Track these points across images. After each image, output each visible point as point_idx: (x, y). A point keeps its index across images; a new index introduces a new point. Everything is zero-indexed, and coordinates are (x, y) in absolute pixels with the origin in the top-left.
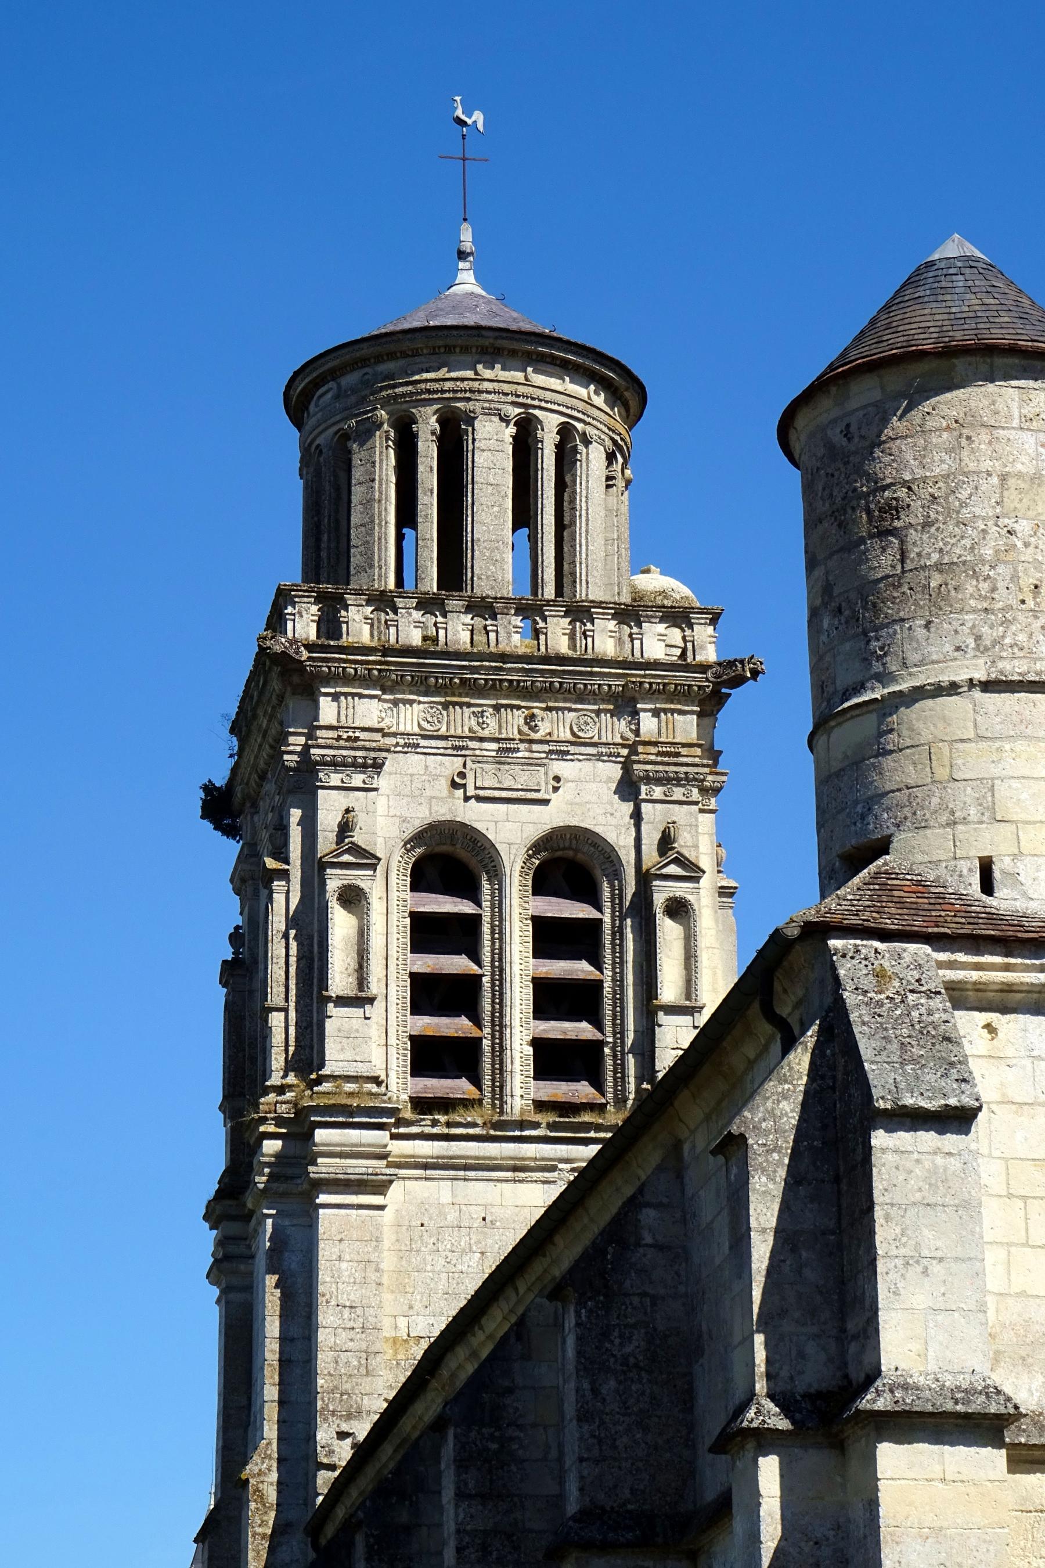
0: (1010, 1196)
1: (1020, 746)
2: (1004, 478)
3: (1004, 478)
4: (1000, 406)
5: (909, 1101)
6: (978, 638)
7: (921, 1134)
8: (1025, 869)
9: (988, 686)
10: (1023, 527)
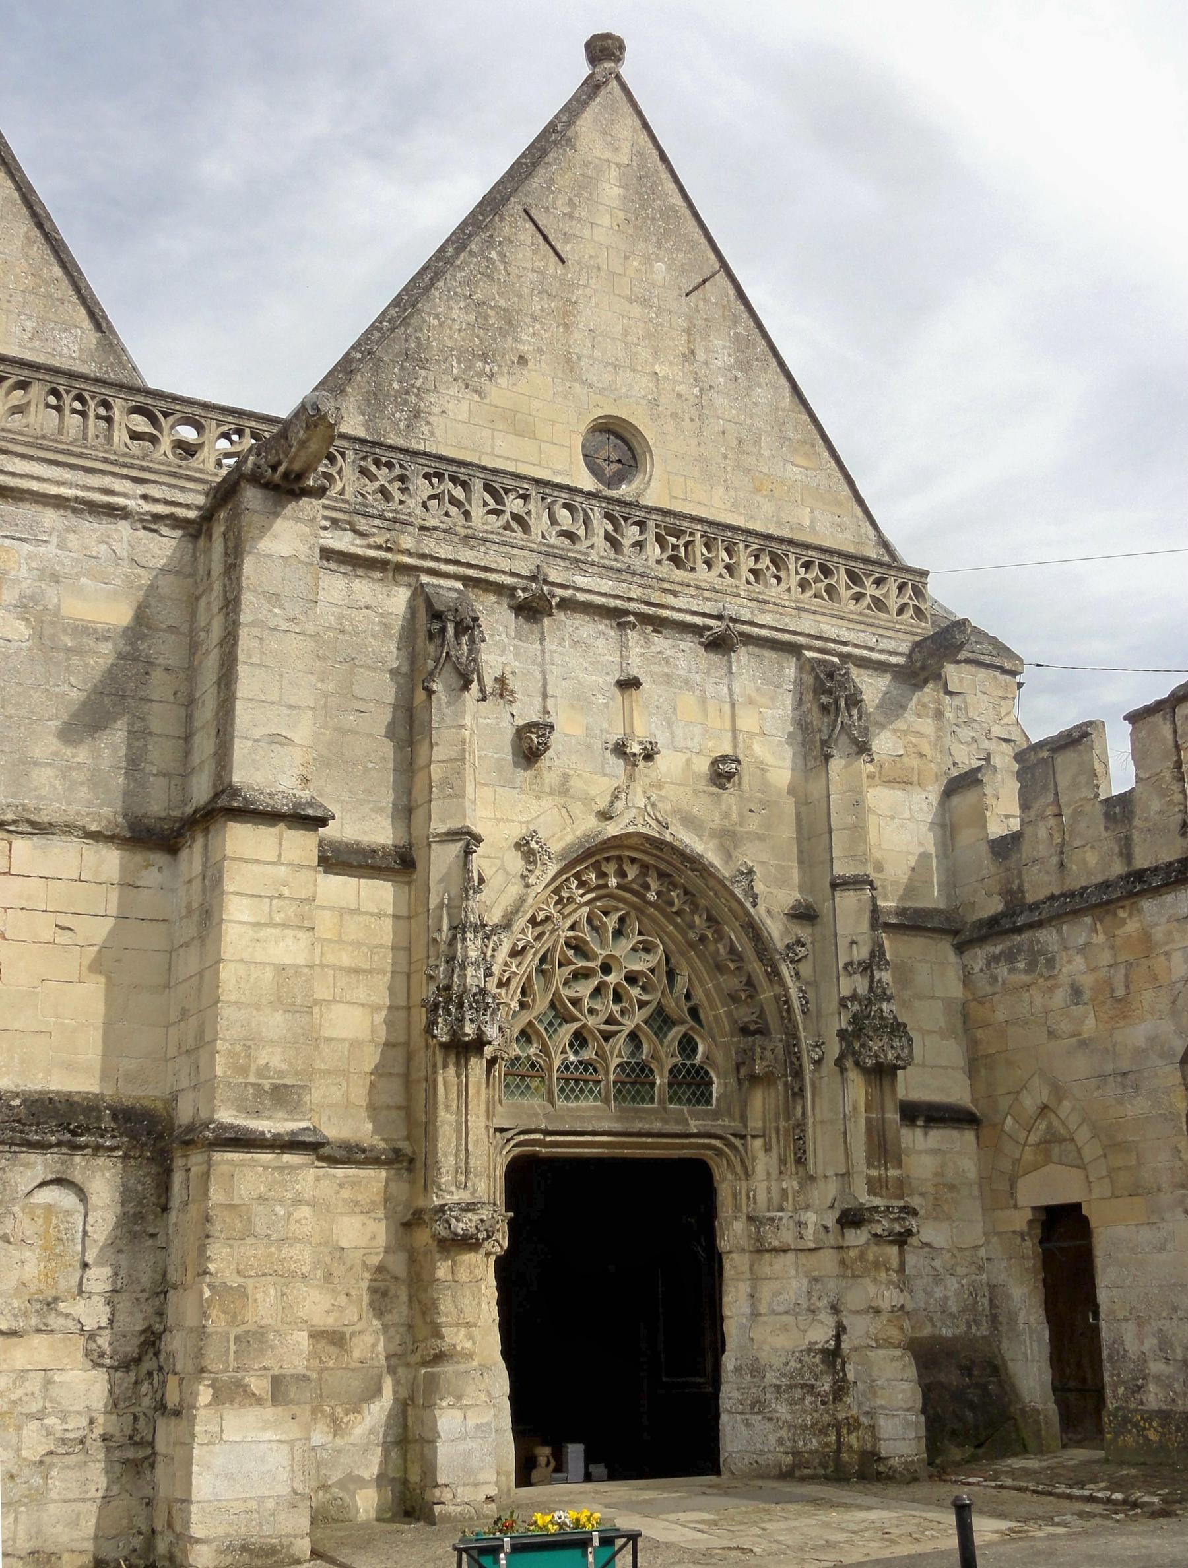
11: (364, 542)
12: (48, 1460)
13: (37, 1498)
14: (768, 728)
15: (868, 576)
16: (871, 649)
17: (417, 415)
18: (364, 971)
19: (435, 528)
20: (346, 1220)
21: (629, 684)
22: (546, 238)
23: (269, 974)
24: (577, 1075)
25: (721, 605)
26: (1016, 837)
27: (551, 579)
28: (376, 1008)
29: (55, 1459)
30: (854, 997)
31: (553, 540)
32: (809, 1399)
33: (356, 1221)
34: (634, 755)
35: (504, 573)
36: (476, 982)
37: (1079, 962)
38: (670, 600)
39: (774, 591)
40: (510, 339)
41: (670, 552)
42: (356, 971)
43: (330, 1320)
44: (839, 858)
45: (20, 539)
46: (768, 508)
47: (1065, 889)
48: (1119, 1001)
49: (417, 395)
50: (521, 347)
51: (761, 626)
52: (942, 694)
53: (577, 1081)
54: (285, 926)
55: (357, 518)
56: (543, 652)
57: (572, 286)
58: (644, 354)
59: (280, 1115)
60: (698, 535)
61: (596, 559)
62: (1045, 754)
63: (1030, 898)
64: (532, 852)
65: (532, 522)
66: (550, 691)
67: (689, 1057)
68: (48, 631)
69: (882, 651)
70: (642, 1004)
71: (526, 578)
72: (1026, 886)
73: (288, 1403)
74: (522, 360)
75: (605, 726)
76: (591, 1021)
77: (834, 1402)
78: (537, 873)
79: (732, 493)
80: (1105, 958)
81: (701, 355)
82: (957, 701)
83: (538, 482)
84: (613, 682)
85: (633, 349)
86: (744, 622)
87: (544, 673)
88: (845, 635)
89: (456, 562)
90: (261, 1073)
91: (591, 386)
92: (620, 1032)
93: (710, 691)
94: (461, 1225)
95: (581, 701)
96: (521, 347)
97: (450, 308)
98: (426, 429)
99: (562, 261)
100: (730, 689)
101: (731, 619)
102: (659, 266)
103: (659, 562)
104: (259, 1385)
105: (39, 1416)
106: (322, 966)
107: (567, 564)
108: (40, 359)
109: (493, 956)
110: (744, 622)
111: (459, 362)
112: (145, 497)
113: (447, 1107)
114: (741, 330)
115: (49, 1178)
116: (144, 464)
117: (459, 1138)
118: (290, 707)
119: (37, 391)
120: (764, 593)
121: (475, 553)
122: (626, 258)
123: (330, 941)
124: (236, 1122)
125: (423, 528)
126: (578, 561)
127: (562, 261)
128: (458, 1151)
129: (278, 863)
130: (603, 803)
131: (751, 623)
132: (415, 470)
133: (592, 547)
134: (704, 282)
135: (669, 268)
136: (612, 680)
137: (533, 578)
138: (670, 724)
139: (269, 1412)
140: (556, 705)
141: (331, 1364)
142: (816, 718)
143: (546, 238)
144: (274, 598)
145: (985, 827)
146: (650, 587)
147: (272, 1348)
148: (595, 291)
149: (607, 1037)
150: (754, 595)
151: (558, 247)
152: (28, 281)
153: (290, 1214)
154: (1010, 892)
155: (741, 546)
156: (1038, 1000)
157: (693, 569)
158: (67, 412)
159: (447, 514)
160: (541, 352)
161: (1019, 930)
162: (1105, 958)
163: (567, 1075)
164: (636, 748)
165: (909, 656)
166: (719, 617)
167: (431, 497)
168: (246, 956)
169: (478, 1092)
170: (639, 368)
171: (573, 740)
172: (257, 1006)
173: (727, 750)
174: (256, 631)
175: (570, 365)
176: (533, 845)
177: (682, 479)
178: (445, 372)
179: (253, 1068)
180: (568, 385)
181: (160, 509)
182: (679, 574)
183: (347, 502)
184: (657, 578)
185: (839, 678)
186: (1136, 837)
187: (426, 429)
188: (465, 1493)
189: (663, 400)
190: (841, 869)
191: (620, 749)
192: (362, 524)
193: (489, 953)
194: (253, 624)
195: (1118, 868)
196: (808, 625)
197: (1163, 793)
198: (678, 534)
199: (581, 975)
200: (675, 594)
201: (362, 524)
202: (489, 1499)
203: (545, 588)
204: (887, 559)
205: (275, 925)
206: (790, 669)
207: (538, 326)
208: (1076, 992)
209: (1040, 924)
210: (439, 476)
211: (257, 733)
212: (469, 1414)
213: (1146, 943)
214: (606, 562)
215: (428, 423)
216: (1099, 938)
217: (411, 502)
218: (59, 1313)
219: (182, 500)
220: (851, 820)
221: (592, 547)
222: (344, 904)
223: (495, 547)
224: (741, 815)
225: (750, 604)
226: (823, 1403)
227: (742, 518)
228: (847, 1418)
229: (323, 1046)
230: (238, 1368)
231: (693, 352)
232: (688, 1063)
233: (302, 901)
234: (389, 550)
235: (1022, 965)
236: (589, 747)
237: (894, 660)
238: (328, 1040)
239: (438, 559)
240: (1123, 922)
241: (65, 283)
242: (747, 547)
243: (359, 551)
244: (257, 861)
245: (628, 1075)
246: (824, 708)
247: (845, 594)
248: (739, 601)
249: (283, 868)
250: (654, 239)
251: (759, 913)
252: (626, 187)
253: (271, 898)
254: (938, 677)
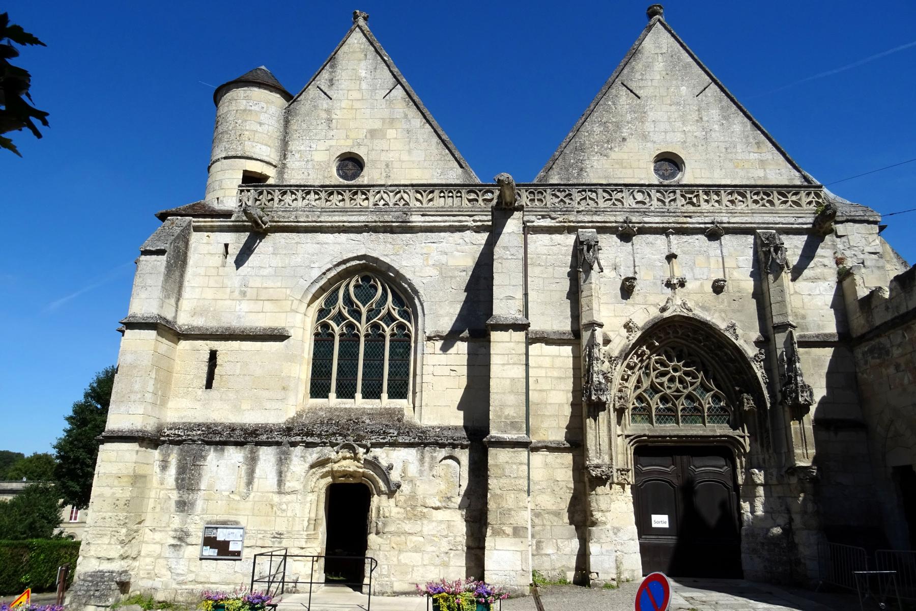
0: (205, 276)
1: (230, 171)
2: (237, 111)
3: (237, 111)
4: (239, 95)
5: (148, 248)
6: (225, 148)
7: (153, 256)
8: (225, 200)
9: (225, 158)
10: (239, 121)
11: (553, 221)
12: (450, 551)
13: (446, 565)
14: (740, 264)
15: (789, 193)
16: (793, 224)
17: (581, 170)
18: (563, 378)
19: (582, 211)
20: (559, 470)
21: (671, 257)
22: (631, 91)
23: (508, 381)
24: (664, 413)
25: (713, 218)
27: (633, 221)
28: (567, 391)
29: (452, 551)
31: (634, 206)
32: (776, 549)
33: (564, 471)
34: (675, 284)
35: (613, 222)
36: (598, 379)
38: (689, 220)
39: (741, 207)
40: (618, 133)
41: (688, 201)
42: (560, 378)
43: (554, 508)
44: (775, 316)
45: (434, 243)
46: (742, 173)
49: (581, 162)
50: (623, 135)
51: (734, 223)
52: (835, 237)
53: (665, 416)
54: (514, 364)
55: (551, 213)
56: (633, 250)
57: (644, 106)
58: (679, 124)
59: (514, 432)
60: (701, 191)
61: (653, 209)
64: (630, 328)
65: (624, 201)
66: (636, 264)
67: (717, 404)
68: (444, 271)
69: (798, 224)
70: (692, 384)
71: (621, 222)
73: (520, 537)
74: (624, 139)
75: (662, 274)
76: (668, 391)
78: (633, 335)
79: (724, 171)
81: (705, 119)
82: (843, 239)
83: (626, 185)
84: (665, 256)
85: (673, 123)
86: (725, 223)
87: (634, 258)
88: (778, 220)
89: (592, 222)
90: (506, 417)
91: (655, 142)
92: (682, 395)
93: (712, 253)
94: (594, 473)
95: (651, 266)
96: (623, 135)
97: (593, 127)
98: (585, 174)
99: (639, 98)
100: (721, 252)
101: (718, 223)
102: (683, 89)
103: (683, 206)
104: (509, 530)
105: (446, 537)
106: (546, 377)
107: (640, 214)
108: (444, 182)
109: (615, 369)
110: (725, 223)
111: (598, 146)
112: (474, 221)
113: (591, 428)
114: (723, 103)
115: (447, 455)
116: (473, 209)
117: (596, 439)
118: (514, 286)
119: (437, 192)
120: (735, 209)
121: (600, 217)
122: (668, 89)
123: (549, 368)
124: (499, 435)
125: (578, 212)
126: (644, 212)
127: (639, 98)
128: (596, 444)
129: (511, 341)
130: (662, 304)
131: (729, 223)
132: (574, 191)
133: (651, 205)
134: (705, 89)
135: (688, 87)
136: (664, 256)
137: (625, 222)
138: (692, 270)
139: (513, 540)
140: (639, 269)
141: (555, 524)
143: (631, 91)
144: (506, 248)
146: (678, 216)
147: (513, 517)
148: (655, 105)
149: (677, 398)
150: (729, 211)
151: (637, 92)
152: (439, 157)
153: (518, 468)
155: (722, 192)
157: (699, 206)
158: (446, 198)
159: (588, 204)
160: (632, 134)
163: (660, 413)
164: (675, 281)
165: (814, 224)
166: (713, 223)
167: (581, 200)
168: (500, 376)
169: (603, 421)
170: (676, 130)
171: (648, 282)
172: (504, 393)
173: (721, 277)
174: (500, 261)
175: (644, 137)
176: (631, 324)
177: (699, 170)
178: (592, 151)
179: (503, 415)
180: (644, 144)
181: (479, 224)
182: (691, 208)
183: (548, 208)
184: (681, 212)
187: (585, 174)
188: (602, 576)
189: (688, 140)
190: (777, 320)
191: (669, 284)
192: (553, 215)
193: (613, 368)
194: (499, 258)
196: (758, 219)
198: (692, 193)
199: (663, 374)
200: (690, 217)
201: (553, 215)
202: (613, 580)
203: (631, 225)
204: (806, 184)
205: (510, 364)
206: (751, 239)
207: (630, 125)
210: (585, 191)
211: (501, 297)
212: (603, 545)
214: (658, 210)
215: (586, 172)
217: (573, 203)
218: (452, 502)
219: (486, 219)
220: (779, 299)
221: (651, 205)
222: (554, 354)
223: (608, 213)
224: (729, 303)
225: (727, 215)
227: (730, 180)
229: (548, 407)
230: (500, 524)
231: (701, 118)
232: (717, 406)
233: (520, 354)
234: (565, 222)
235: (876, 355)
236: (655, 284)
237: (805, 226)
238: (550, 404)
239: (585, 222)
241: (450, 155)
242: (725, 192)
243: (553, 225)
244: (503, 342)
245: (688, 412)
247: (776, 202)
248: (722, 214)
249: (512, 344)
250: (680, 78)
251: (740, 343)
252: (666, 61)
253: (508, 354)
254: (831, 231)
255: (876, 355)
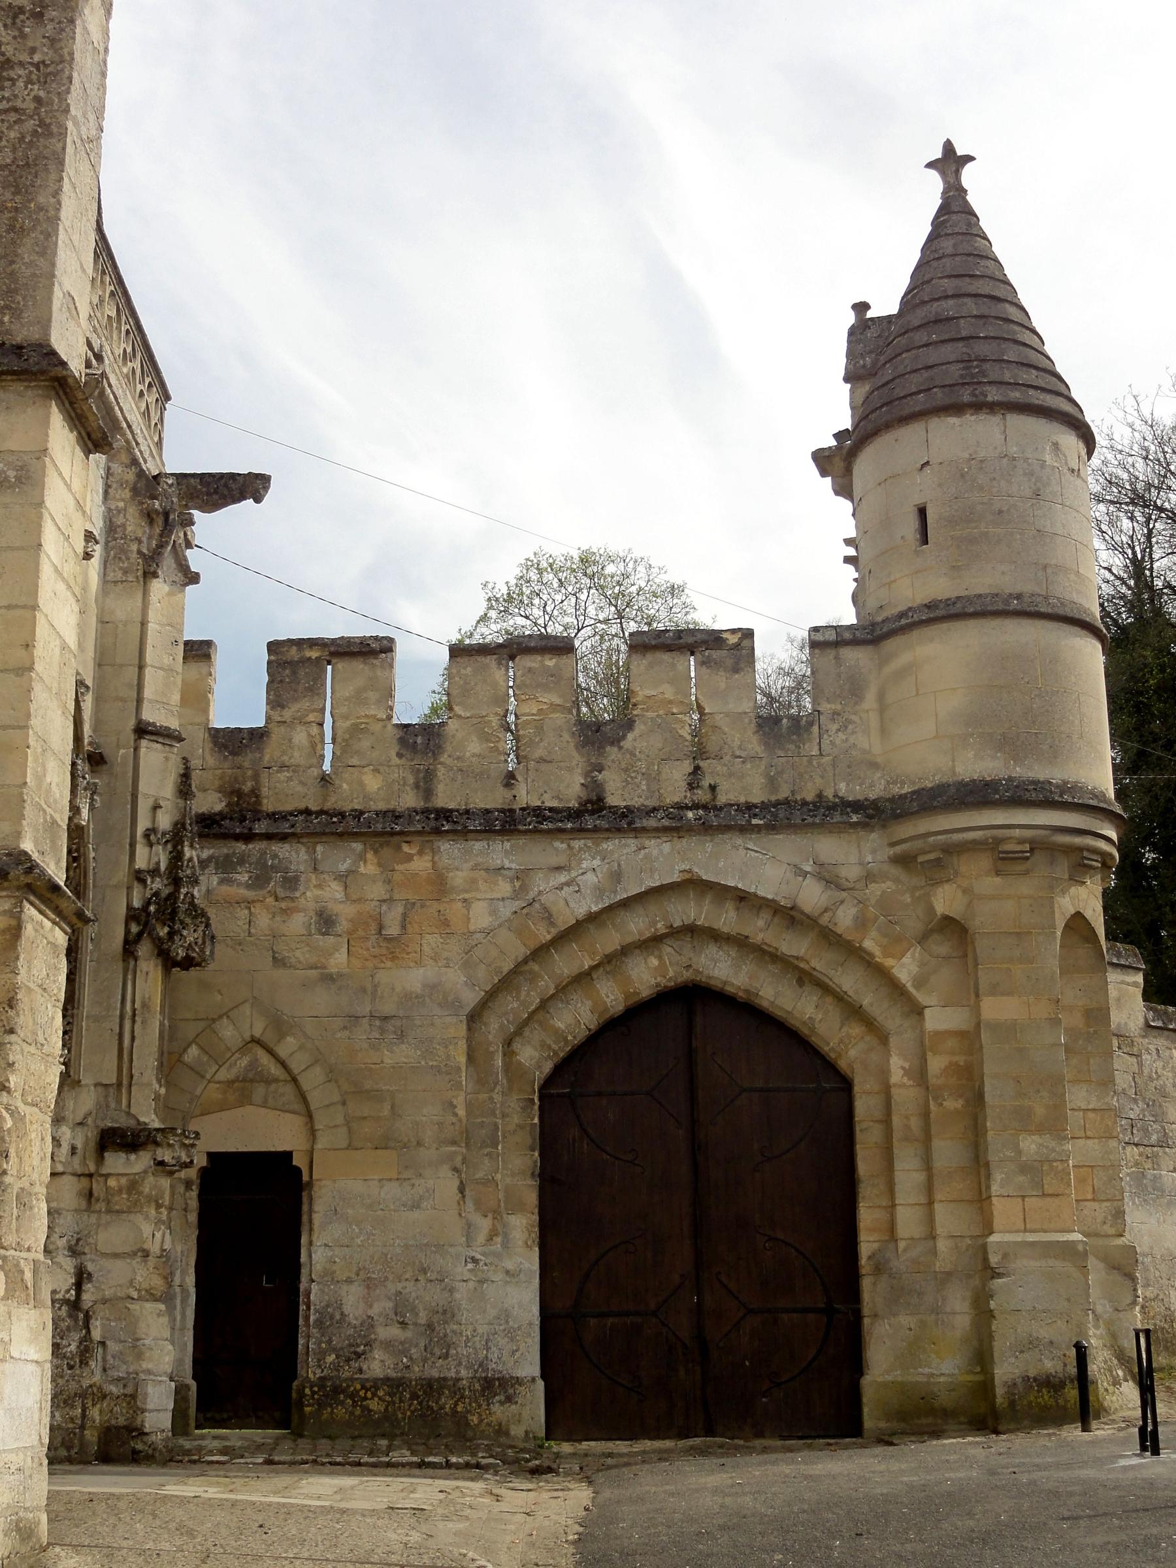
26: (256, 736)
30: (155, 872)
37: (335, 890)
44: (150, 701)
47: (328, 806)
48: (389, 939)
62: (314, 654)
63: (268, 805)
72: (265, 791)
77: (80, 1367)
80: (377, 891)
142: (133, 524)
145: (205, 711)
154: (239, 793)
156: (263, 920)
161: (248, 837)
162: (377, 891)
185: (165, 487)
186: (441, 772)
195: (410, 800)
197: (485, 737)
208: (326, 921)
209: (284, 838)
213: (440, 885)
216: (369, 868)
226: (71, 1367)
228: (91, 1386)
235: (244, 878)
240: (409, 858)
246: (149, 516)
255: (244, 878)
